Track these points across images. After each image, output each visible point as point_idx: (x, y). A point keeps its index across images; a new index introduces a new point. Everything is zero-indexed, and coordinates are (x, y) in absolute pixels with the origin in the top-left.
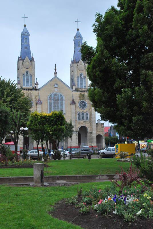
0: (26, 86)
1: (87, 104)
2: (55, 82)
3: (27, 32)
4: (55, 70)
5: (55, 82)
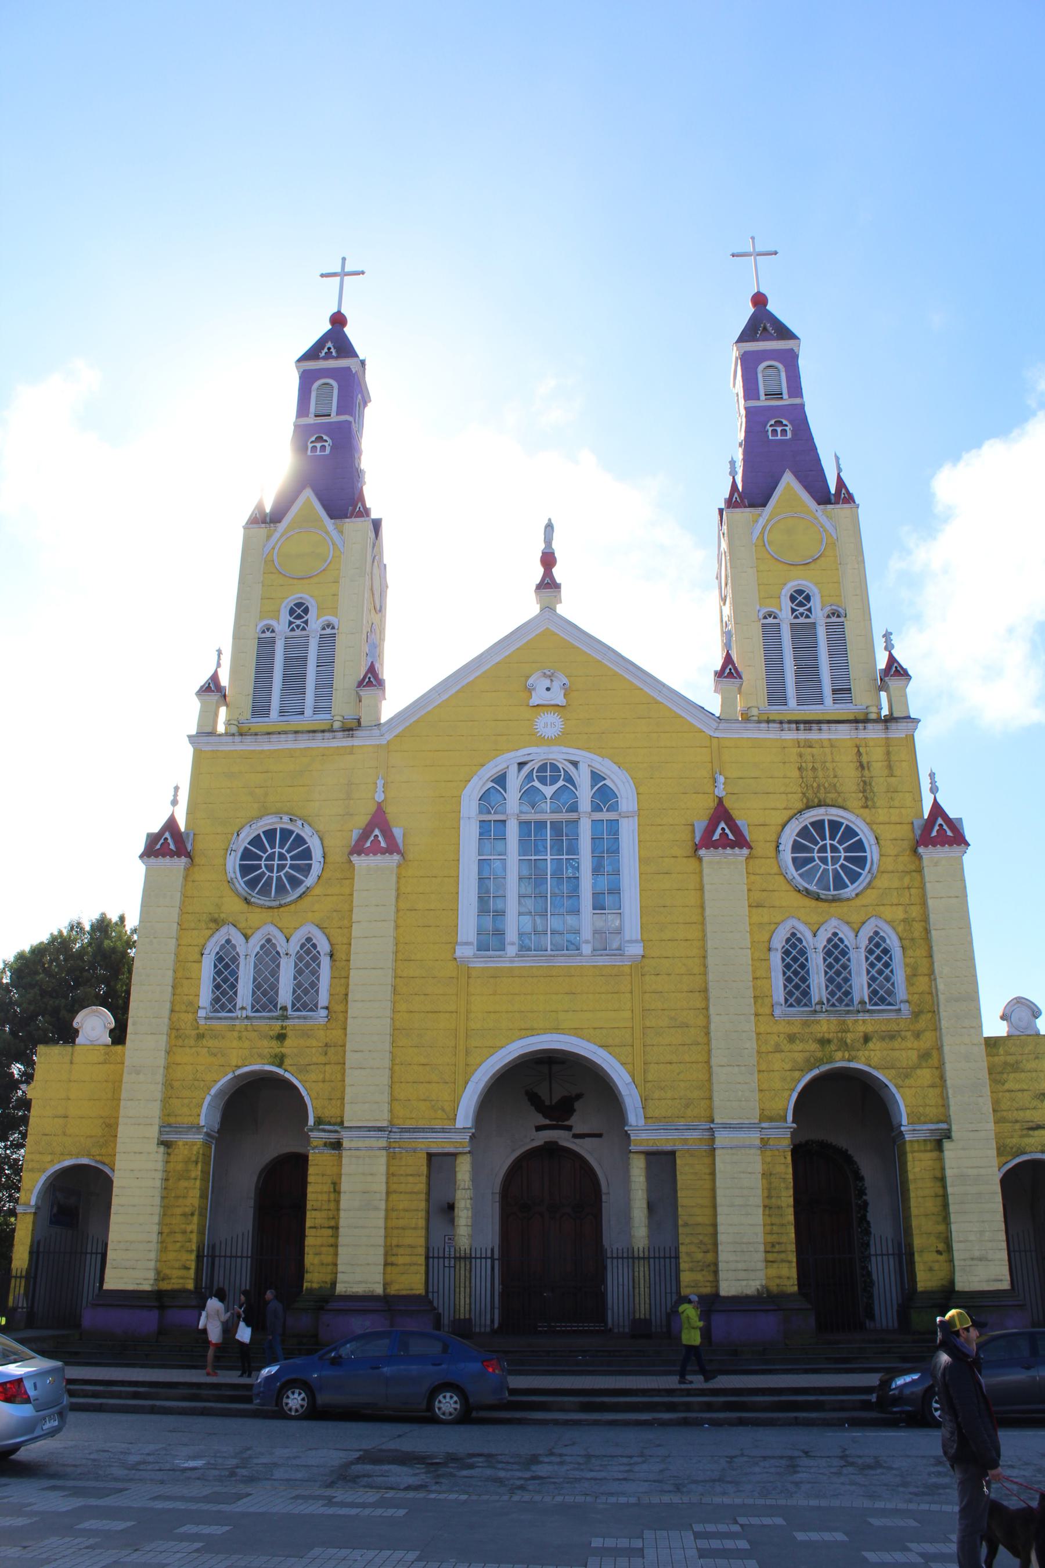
0: (282, 712)
1: (872, 852)
3: (345, 349)
4: (548, 560)
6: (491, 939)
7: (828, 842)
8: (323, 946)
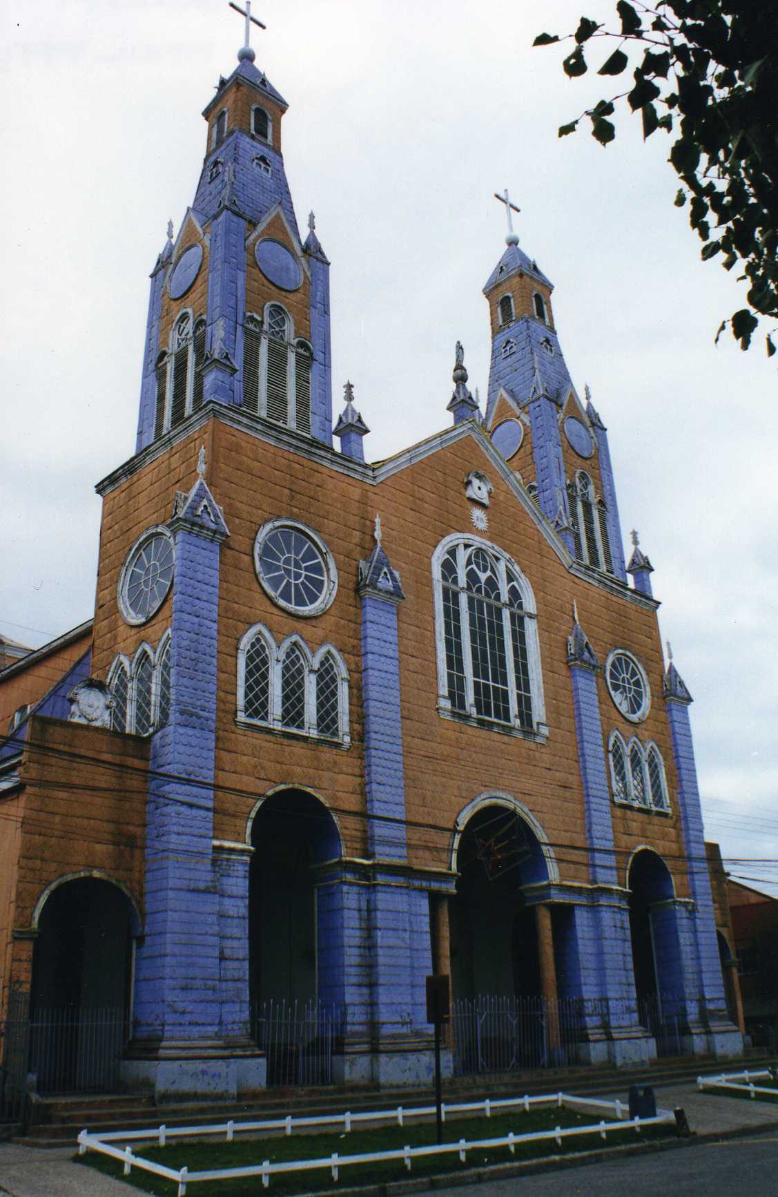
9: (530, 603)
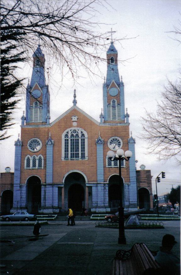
2: (75, 112)
4: (75, 97)
5: (75, 112)
6: (66, 156)
7: (115, 142)
8: (43, 158)
9: (86, 136)
